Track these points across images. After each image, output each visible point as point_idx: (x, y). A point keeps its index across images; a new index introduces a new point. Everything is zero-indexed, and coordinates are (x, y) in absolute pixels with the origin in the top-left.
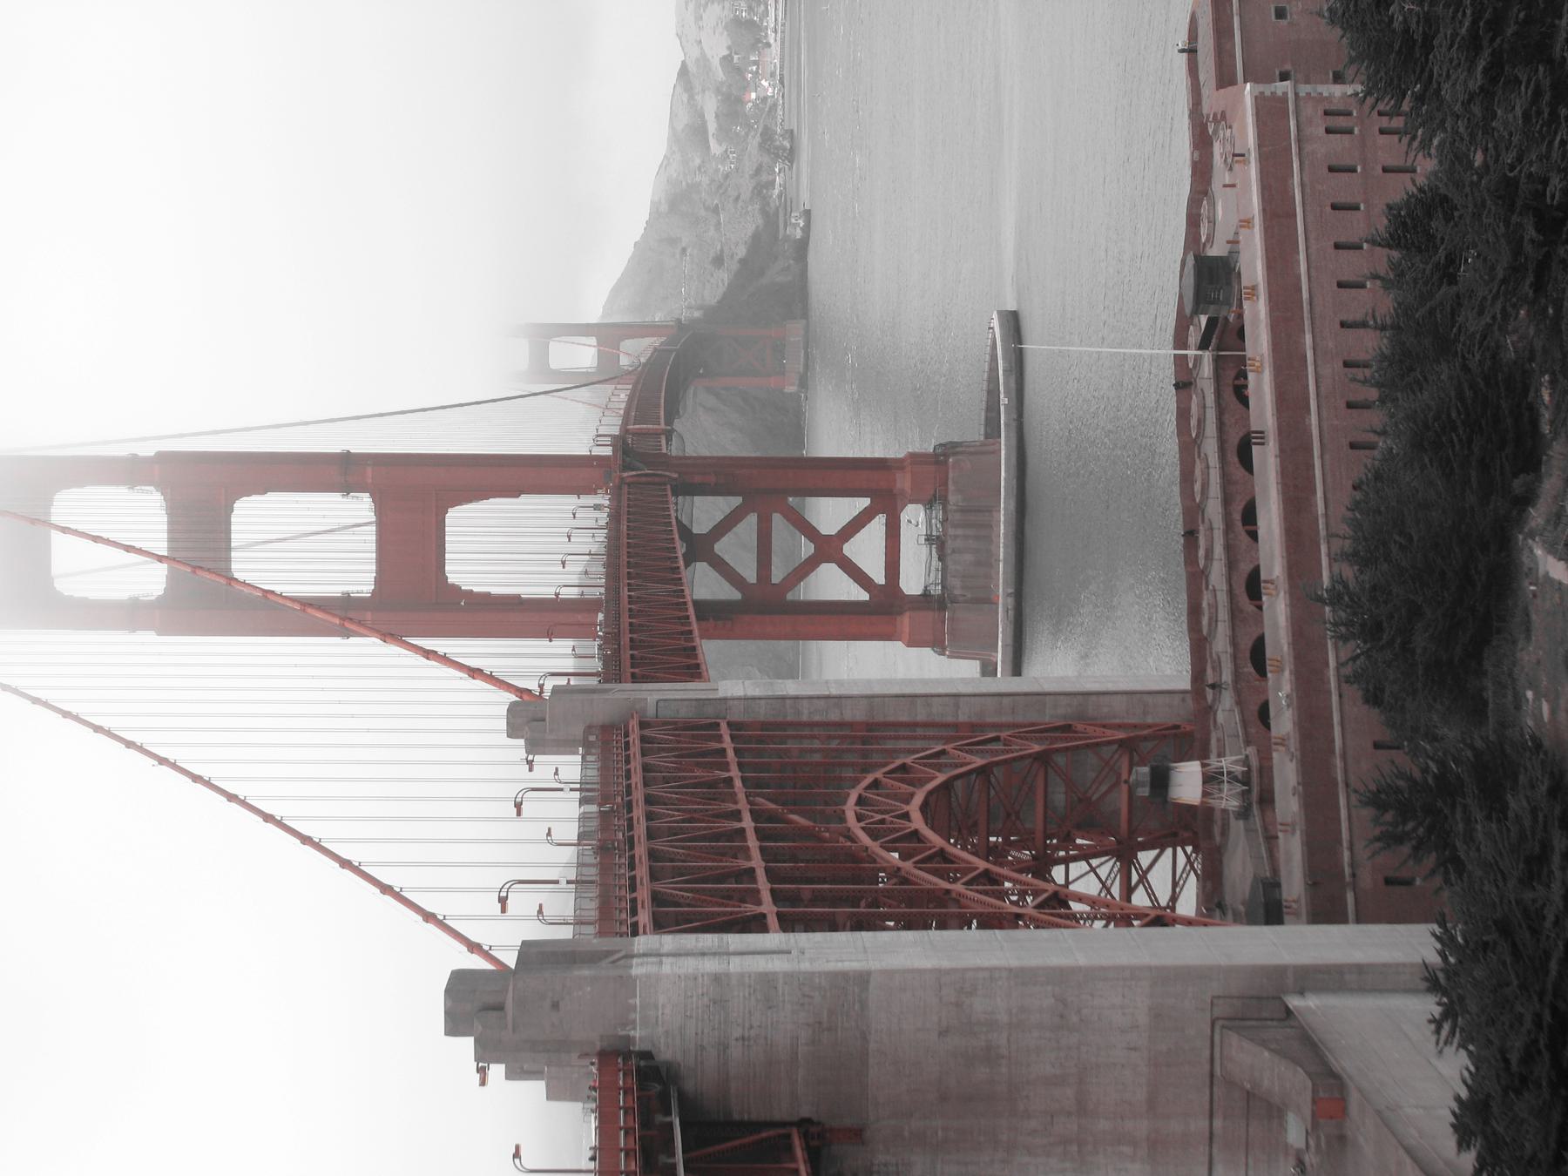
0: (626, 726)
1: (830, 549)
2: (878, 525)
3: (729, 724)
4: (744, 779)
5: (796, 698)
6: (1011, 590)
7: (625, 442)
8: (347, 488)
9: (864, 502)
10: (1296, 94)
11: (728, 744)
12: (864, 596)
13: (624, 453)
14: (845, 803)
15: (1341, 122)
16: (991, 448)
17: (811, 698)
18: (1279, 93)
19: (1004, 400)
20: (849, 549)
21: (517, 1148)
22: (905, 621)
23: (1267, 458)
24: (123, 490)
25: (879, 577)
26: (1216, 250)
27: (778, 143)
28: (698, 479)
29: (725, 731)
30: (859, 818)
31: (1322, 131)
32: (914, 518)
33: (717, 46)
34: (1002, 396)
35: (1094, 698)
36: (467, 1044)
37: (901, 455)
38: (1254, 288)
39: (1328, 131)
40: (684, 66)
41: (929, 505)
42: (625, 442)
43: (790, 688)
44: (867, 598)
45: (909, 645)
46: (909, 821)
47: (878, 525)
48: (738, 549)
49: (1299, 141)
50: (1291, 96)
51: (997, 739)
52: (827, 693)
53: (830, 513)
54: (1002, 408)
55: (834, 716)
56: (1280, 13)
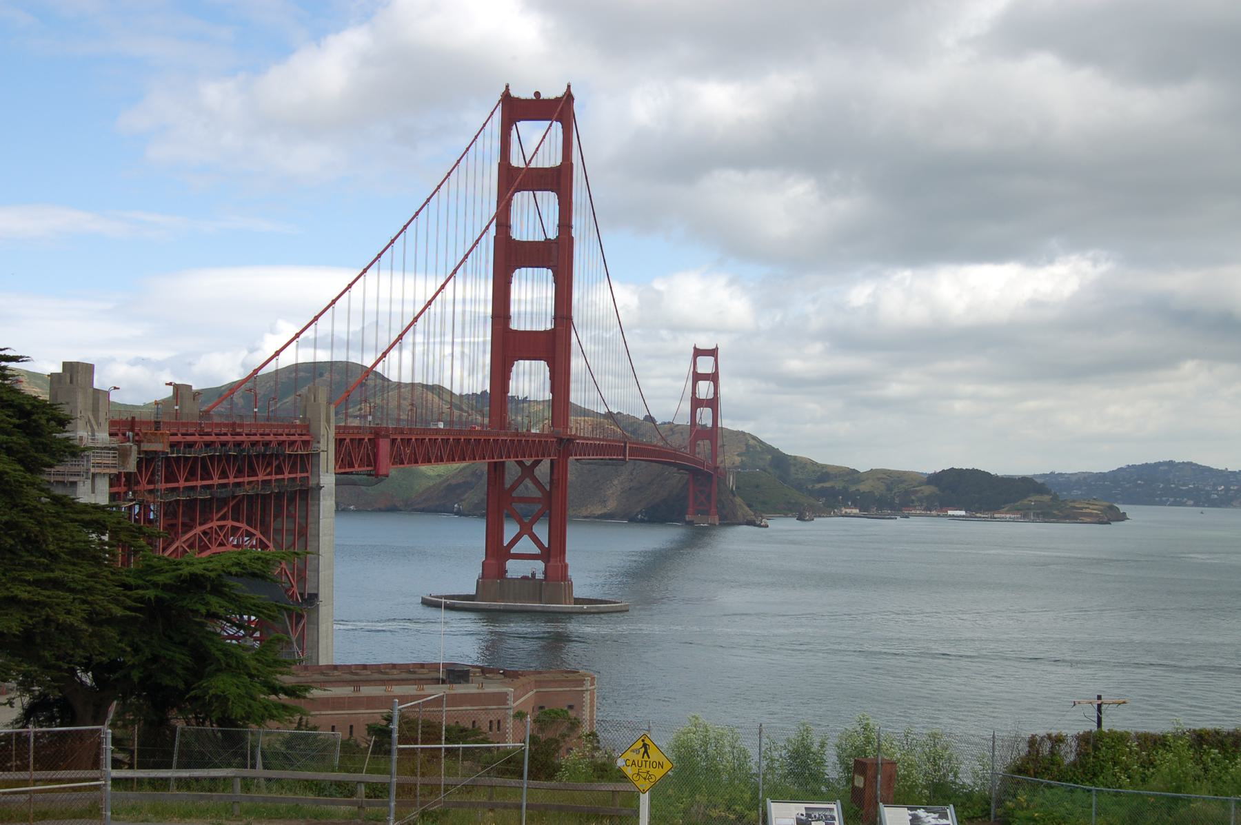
0: (308, 435)
1: (526, 529)
2: (537, 551)
3: (308, 477)
4: (258, 481)
5: (319, 505)
6: (502, 608)
7: (573, 440)
8: (555, 318)
9: (547, 546)
10: (508, 709)
11: (287, 476)
12: (505, 544)
13: (568, 440)
14: (233, 520)
15: (495, 727)
16: (568, 601)
17: (319, 510)
18: (508, 702)
19: (585, 607)
20: (526, 538)
21: (118, 388)
22: (493, 562)
23: (345, 691)
24: (557, 222)
25: (513, 551)
26: (470, 678)
27: (807, 514)
28: (555, 471)
29: (299, 475)
30: (221, 527)
31: (491, 718)
32: (538, 567)
33: (864, 487)
34: (589, 606)
35: (316, 627)
36: (59, 370)
37: (567, 561)
38: (423, 689)
39: (491, 722)
40: (859, 472)
41: (545, 573)
42: (573, 440)
43: (327, 504)
44: (505, 545)
45: (483, 563)
46: (218, 546)
47: (537, 551)
48: (528, 489)
49: (486, 709)
50: (507, 707)
51: (293, 586)
52: (321, 517)
53: (542, 531)
54: (582, 606)
55: (310, 520)
56: (571, 707)
